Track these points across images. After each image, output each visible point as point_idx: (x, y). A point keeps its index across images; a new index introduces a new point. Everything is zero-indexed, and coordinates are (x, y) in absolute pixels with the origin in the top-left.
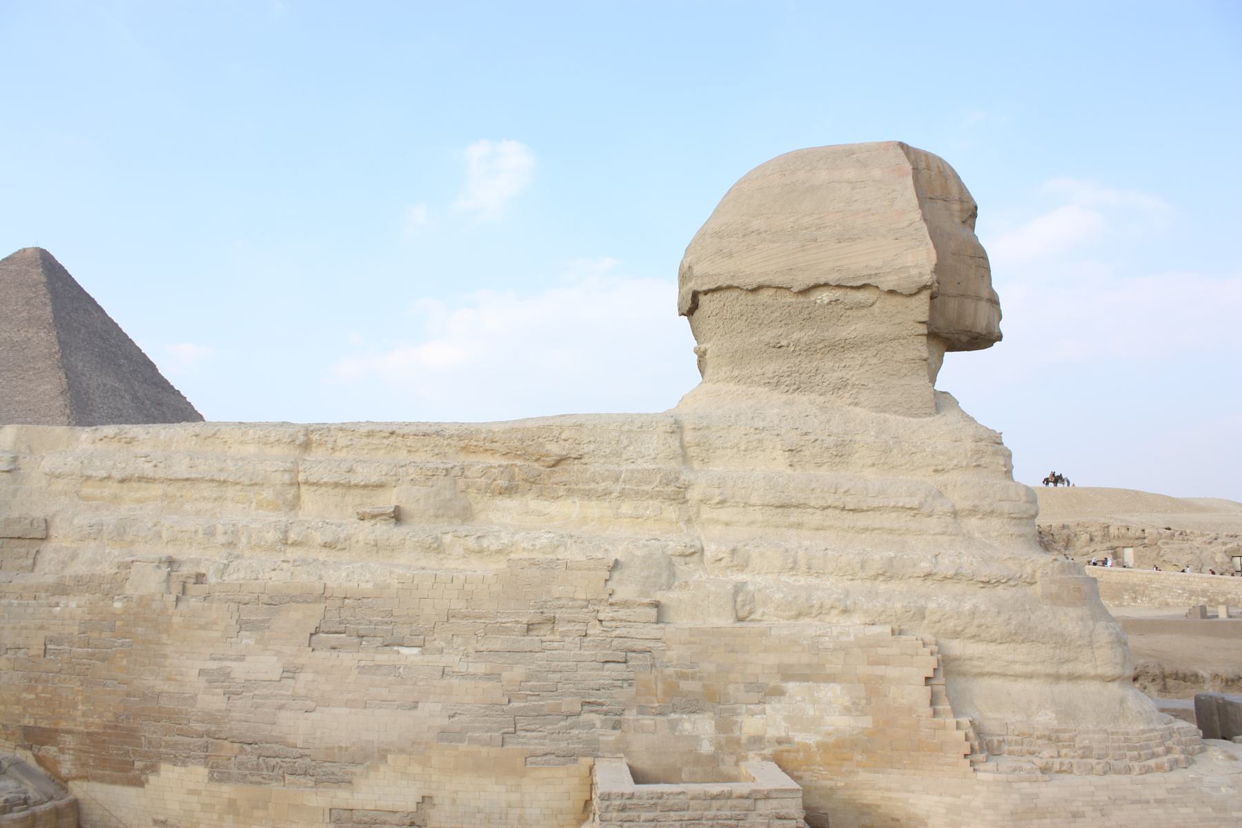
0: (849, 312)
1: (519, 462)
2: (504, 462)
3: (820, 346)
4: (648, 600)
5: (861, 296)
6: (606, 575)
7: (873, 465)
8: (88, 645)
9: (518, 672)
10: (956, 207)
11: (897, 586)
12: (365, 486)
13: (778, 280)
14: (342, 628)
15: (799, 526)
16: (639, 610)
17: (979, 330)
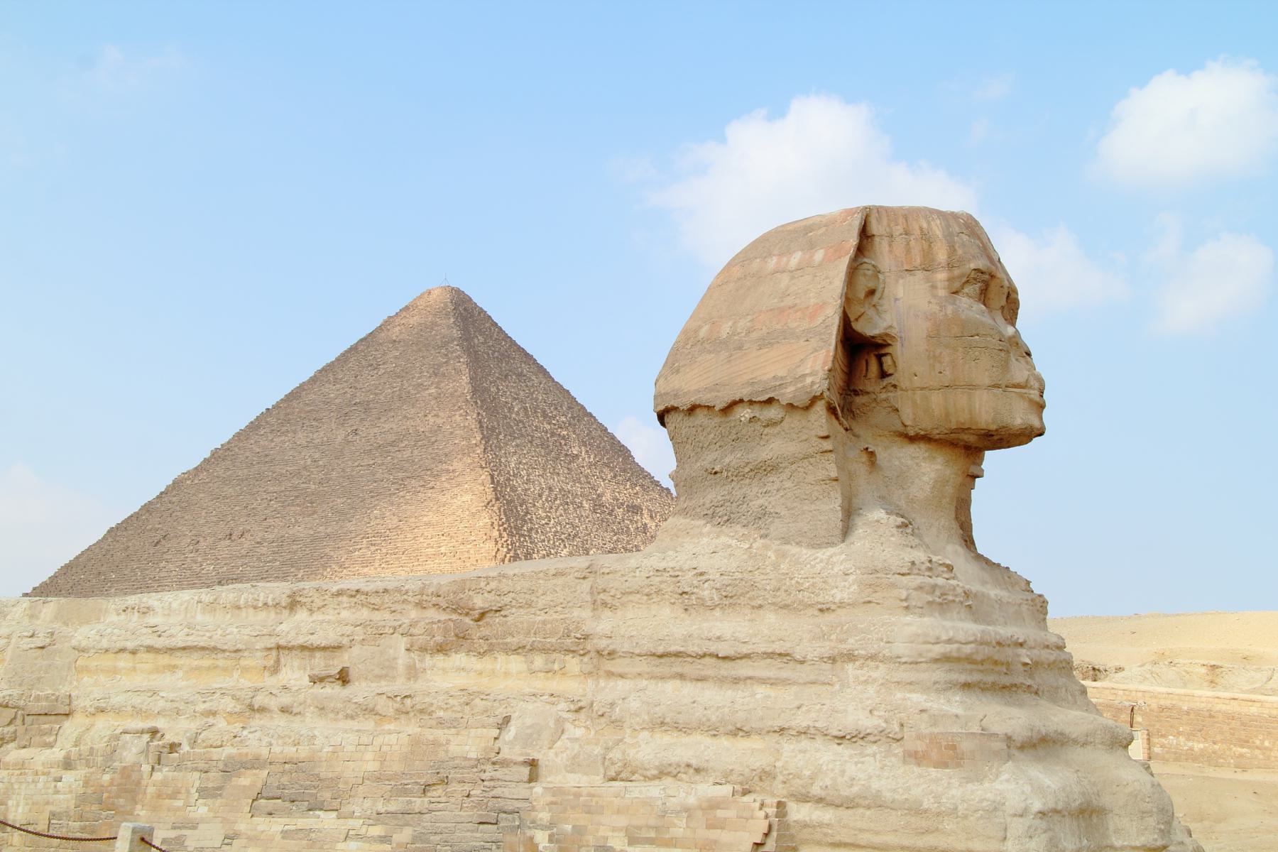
0: (767, 430)
1: (454, 617)
2: (444, 617)
3: (747, 470)
4: (521, 759)
5: (773, 413)
6: (495, 732)
7: (761, 606)
8: (81, 818)
9: (405, 835)
10: (941, 276)
11: (755, 743)
12: (325, 649)
13: (705, 399)
14: (278, 793)
15: (682, 677)
16: (515, 768)
17: (983, 425)
